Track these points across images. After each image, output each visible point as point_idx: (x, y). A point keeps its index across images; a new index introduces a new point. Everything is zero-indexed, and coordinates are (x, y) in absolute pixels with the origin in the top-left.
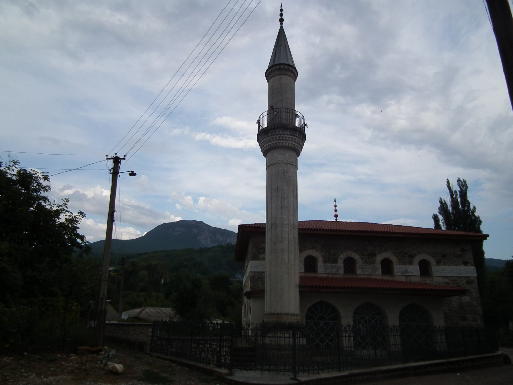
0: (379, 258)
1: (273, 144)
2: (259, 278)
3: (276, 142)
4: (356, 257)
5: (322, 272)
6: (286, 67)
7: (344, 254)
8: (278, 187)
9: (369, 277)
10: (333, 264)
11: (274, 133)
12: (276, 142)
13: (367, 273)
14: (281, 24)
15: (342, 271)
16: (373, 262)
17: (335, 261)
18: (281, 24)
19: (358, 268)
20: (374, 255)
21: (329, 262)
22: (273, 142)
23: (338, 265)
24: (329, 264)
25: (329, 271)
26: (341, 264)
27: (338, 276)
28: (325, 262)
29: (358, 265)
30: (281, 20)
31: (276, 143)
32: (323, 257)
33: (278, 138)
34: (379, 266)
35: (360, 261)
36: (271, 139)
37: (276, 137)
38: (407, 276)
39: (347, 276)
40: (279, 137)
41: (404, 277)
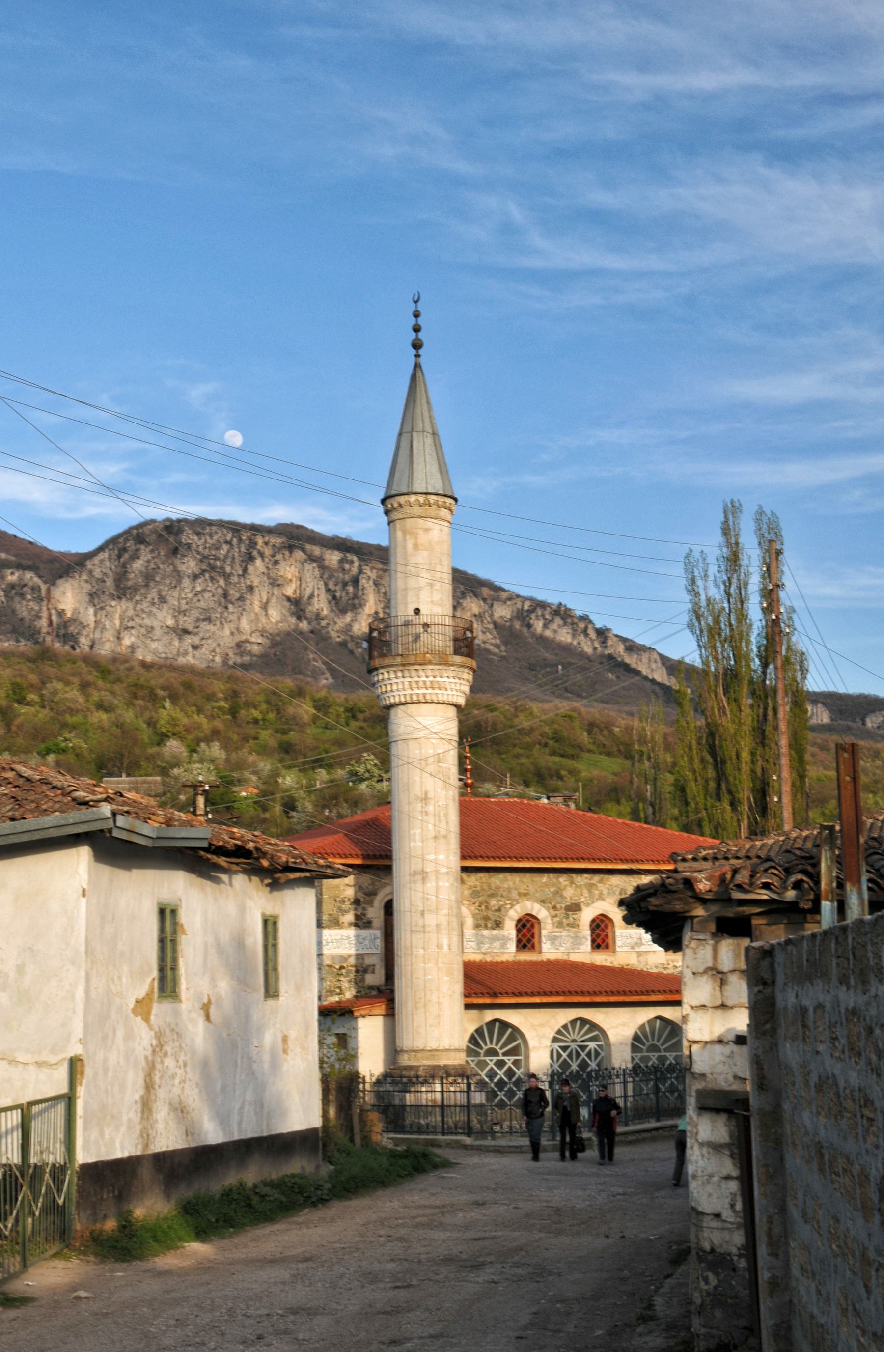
0: (587, 915)
1: (418, 694)
2: (342, 968)
3: (424, 691)
4: (541, 912)
5: (471, 950)
6: (441, 499)
7: (517, 907)
8: (426, 793)
9: (565, 958)
10: (495, 932)
11: (421, 673)
12: (424, 691)
13: (562, 949)
14: (417, 356)
15: (512, 947)
16: (575, 925)
17: (498, 925)
18: (417, 356)
19: (543, 939)
20: (575, 908)
21: (486, 927)
22: (417, 691)
23: (505, 932)
24: (486, 933)
25: (485, 947)
26: (510, 930)
27: (504, 958)
28: (477, 926)
29: (544, 932)
30: (417, 345)
31: (424, 695)
32: (474, 916)
33: (428, 684)
34: (588, 933)
35: (549, 921)
36: (414, 685)
37: (424, 682)
38: (639, 954)
39: (526, 957)
40: (431, 682)
41: (635, 955)
